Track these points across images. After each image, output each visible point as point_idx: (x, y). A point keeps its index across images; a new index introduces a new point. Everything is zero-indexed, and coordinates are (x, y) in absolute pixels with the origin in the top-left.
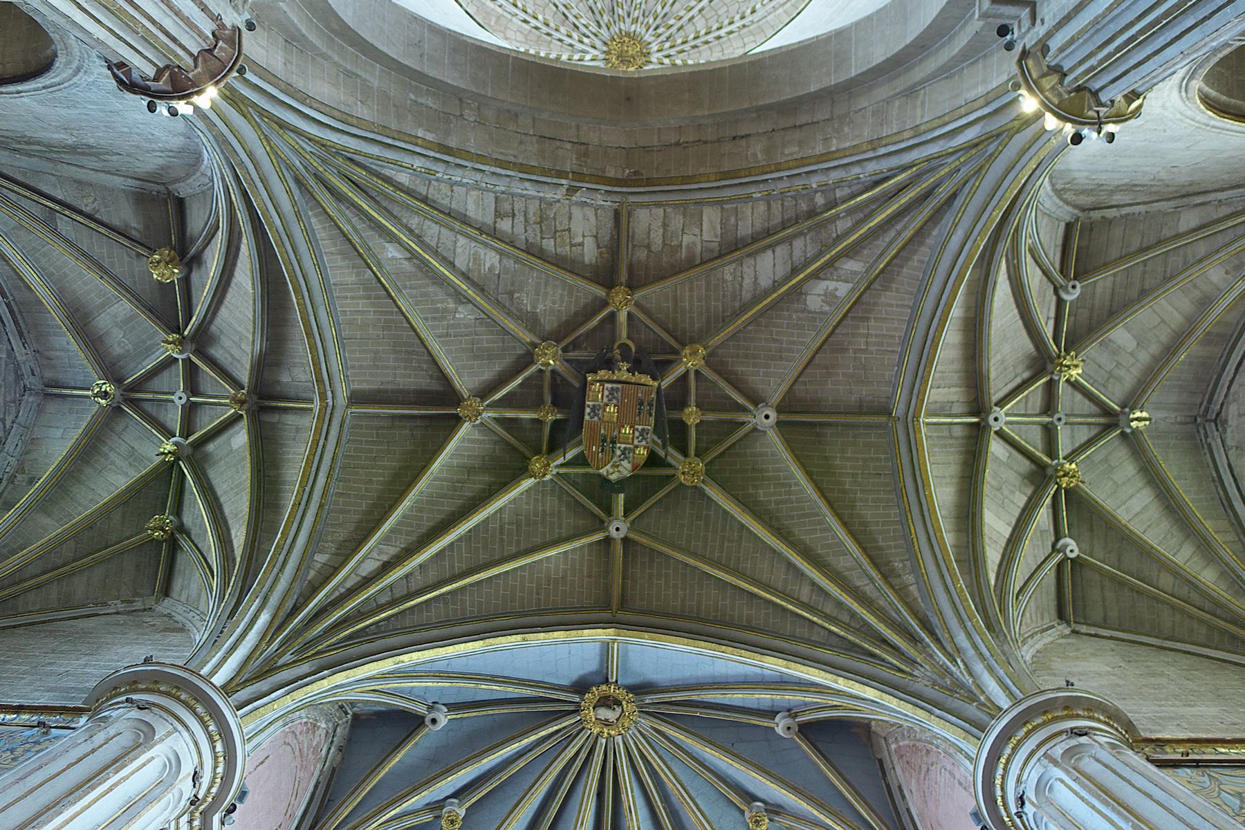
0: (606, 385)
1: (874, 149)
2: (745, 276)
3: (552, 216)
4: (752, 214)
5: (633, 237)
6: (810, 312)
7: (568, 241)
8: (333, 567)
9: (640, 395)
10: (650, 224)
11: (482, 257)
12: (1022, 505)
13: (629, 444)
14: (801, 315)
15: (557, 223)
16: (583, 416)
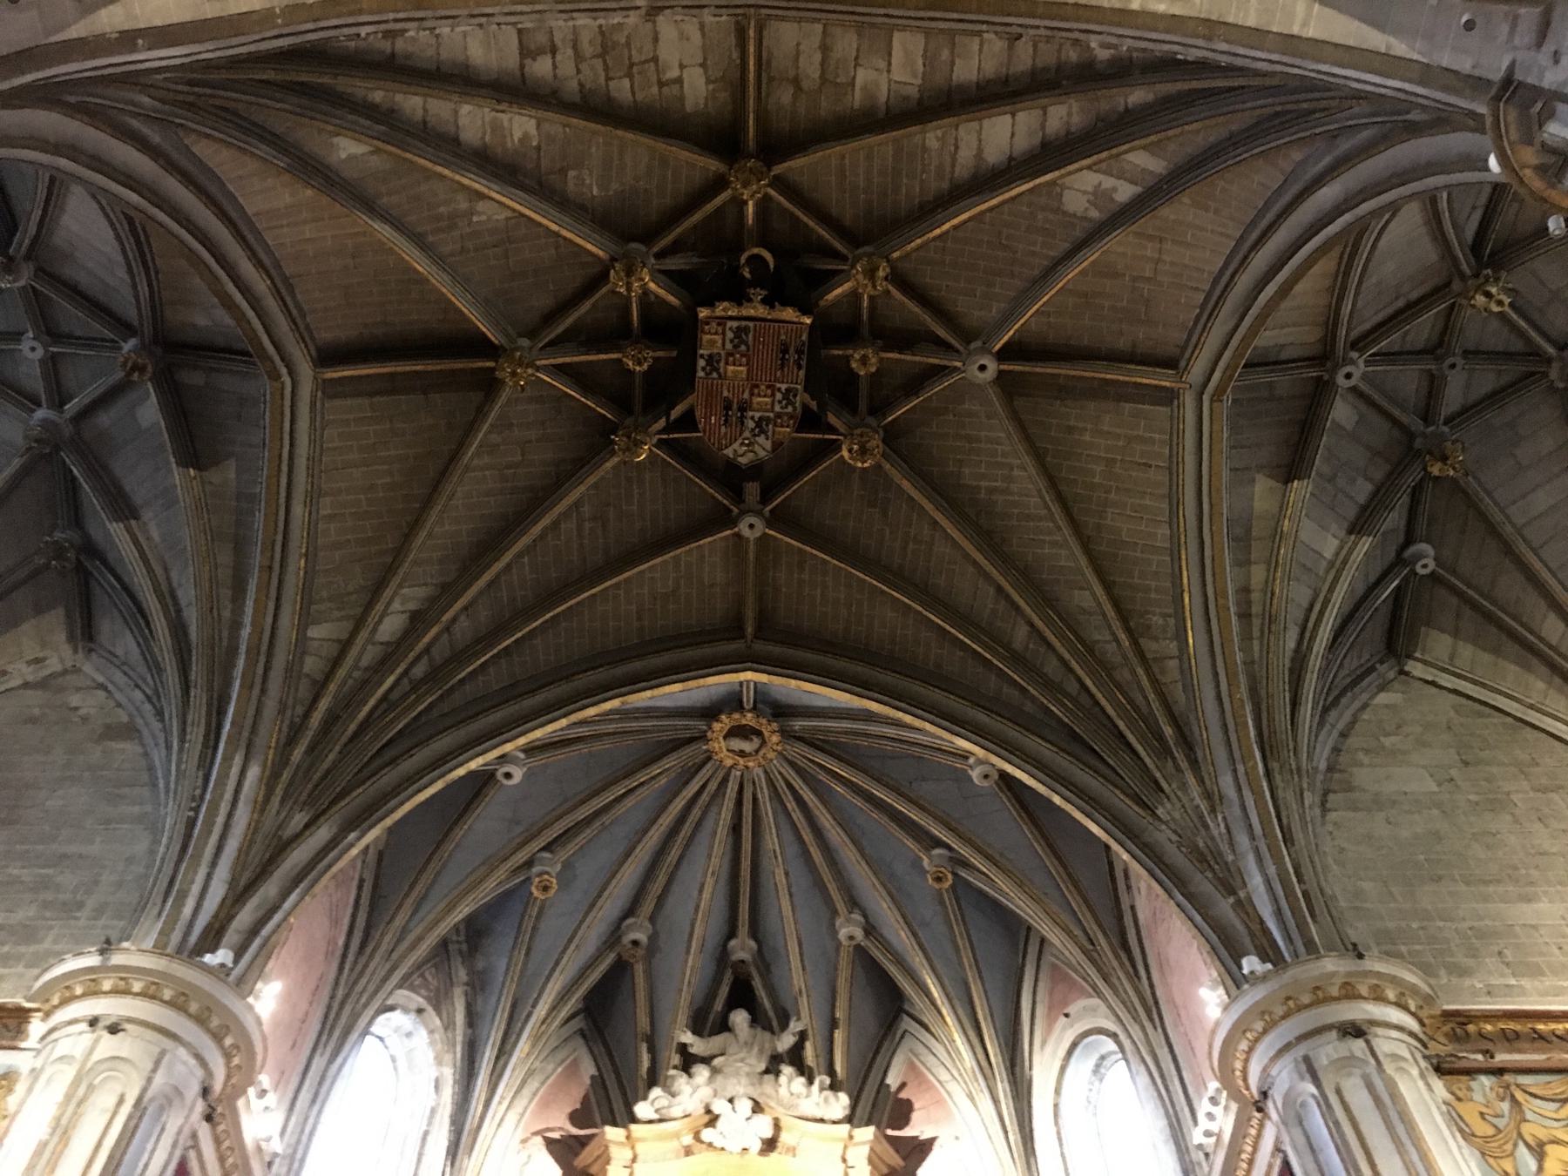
0: (730, 324)
1: (1209, 39)
2: (962, 145)
3: (623, 40)
4: (981, 51)
5: (769, 62)
6: (1065, 213)
7: (654, 79)
8: (339, 641)
9: (783, 337)
10: (798, 44)
11: (506, 124)
12: (1362, 499)
13: (767, 411)
14: (1051, 217)
15: (633, 53)
16: (695, 371)
